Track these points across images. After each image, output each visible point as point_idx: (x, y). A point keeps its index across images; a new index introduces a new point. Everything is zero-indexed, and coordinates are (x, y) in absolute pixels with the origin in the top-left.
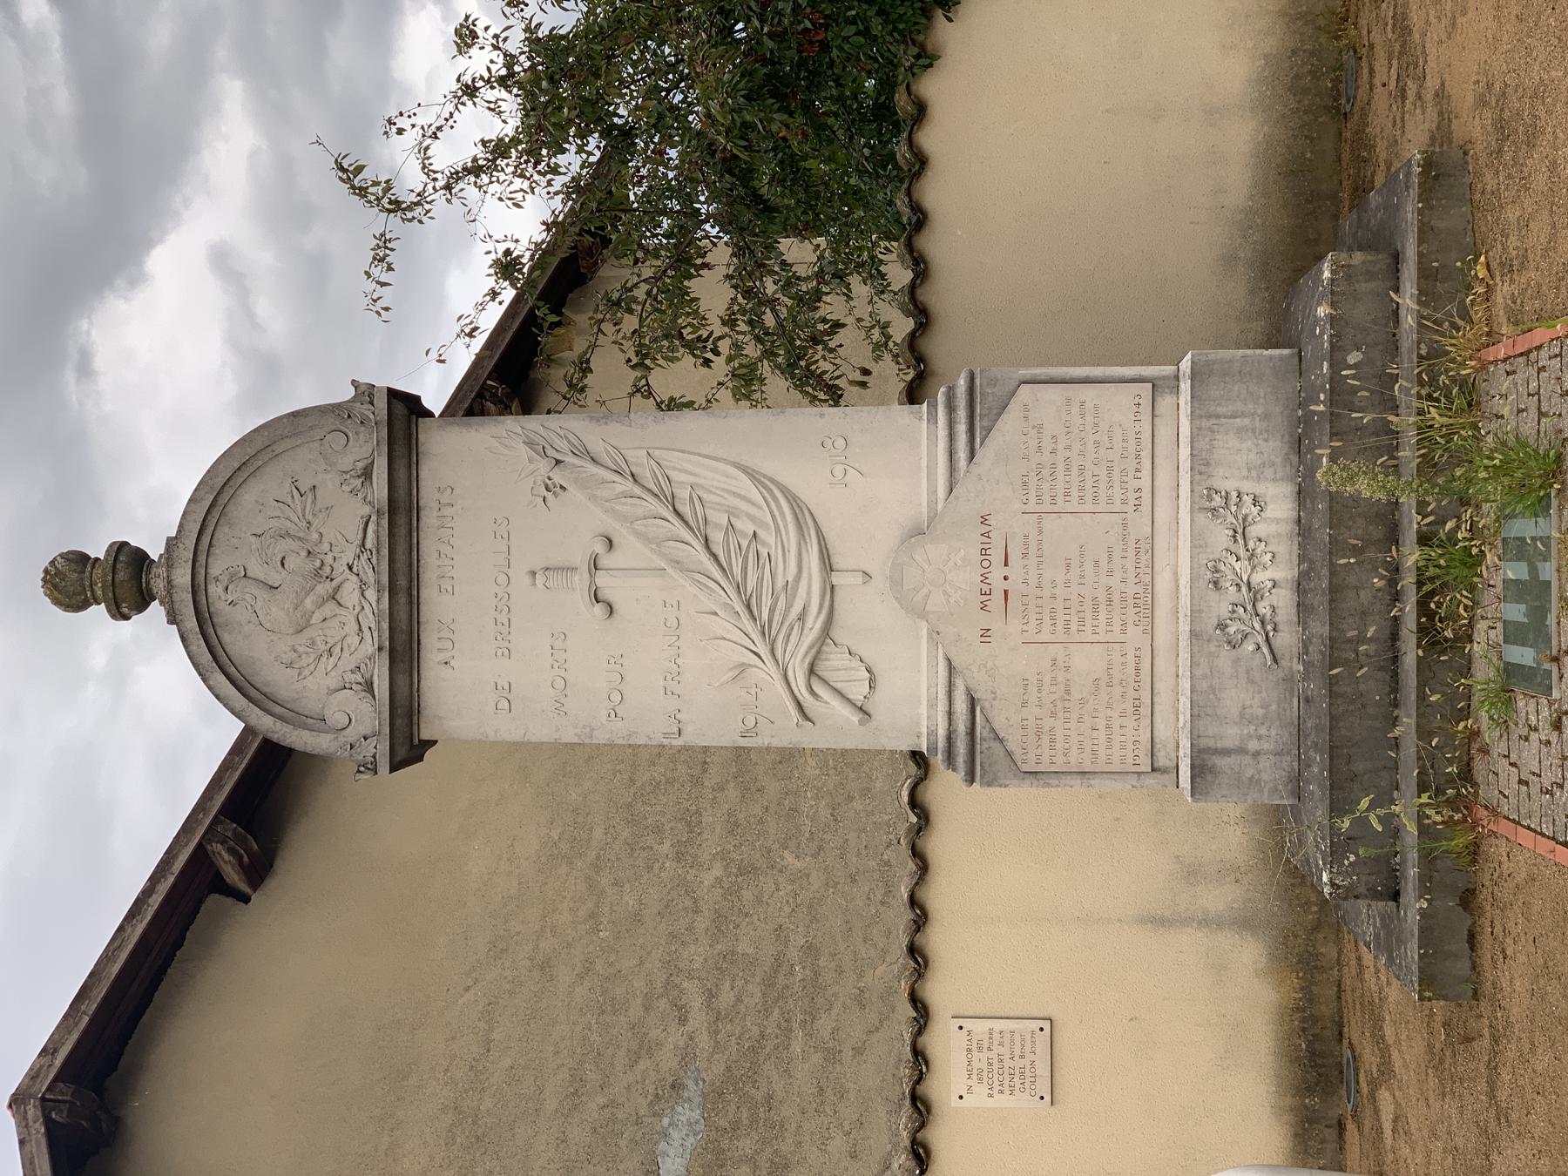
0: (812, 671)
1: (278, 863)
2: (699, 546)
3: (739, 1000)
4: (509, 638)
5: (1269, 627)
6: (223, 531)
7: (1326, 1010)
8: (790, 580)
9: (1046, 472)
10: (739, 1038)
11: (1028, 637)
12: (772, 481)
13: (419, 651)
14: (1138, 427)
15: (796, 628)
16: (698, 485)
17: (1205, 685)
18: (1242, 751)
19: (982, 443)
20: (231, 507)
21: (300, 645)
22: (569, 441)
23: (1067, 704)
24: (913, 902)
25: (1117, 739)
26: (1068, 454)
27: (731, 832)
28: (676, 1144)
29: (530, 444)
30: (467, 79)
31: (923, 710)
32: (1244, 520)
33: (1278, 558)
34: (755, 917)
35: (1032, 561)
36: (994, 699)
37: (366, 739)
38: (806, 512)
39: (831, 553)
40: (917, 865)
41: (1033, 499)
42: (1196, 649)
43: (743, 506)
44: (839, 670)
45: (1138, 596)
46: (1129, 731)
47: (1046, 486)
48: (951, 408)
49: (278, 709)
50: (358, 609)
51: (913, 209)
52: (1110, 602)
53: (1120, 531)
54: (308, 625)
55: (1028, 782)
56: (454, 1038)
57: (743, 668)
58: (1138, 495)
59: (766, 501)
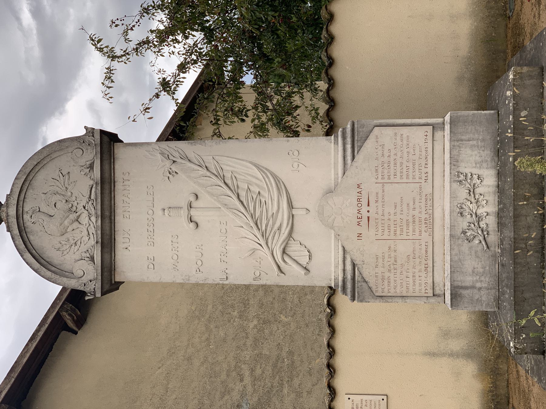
0: (284, 252)
1: (88, 319)
2: (235, 198)
3: (263, 372)
4: (153, 237)
5: (485, 233)
6: (30, 192)
7: (502, 391)
10: (263, 387)
11: (379, 237)
12: (266, 169)
13: (114, 243)
15: (277, 233)
16: (234, 171)
17: (456, 258)
18: (473, 287)
19: (358, 152)
20: (33, 181)
21: (63, 241)
22: (179, 153)
24: (329, 345)
25: (417, 282)
26: (395, 157)
27: (261, 307)
29: (162, 154)
30: (145, 6)
31: (333, 269)
32: (474, 186)
33: (489, 203)
34: (270, 340)
35: (380, 204)
36: (363, 264)
37: (91, 281)
38: (281, 183)
39: (292, 201)
40: (330, 330)
41: (380, 177)
42: (452, 242)
43: (254, 180)
44: (296, 251)
45: (427, 219)
46: (423, 278)
48: (344, 138)
49: (53, 269)
50: (88, 225)
51: (328, 58)
52: (414, 222)
53: (418, 191)
54: (66, 232)
55: (378, 300)
56: (154, 387)
57: (254, 250)
58: (426, 175)
59: (264, 179)
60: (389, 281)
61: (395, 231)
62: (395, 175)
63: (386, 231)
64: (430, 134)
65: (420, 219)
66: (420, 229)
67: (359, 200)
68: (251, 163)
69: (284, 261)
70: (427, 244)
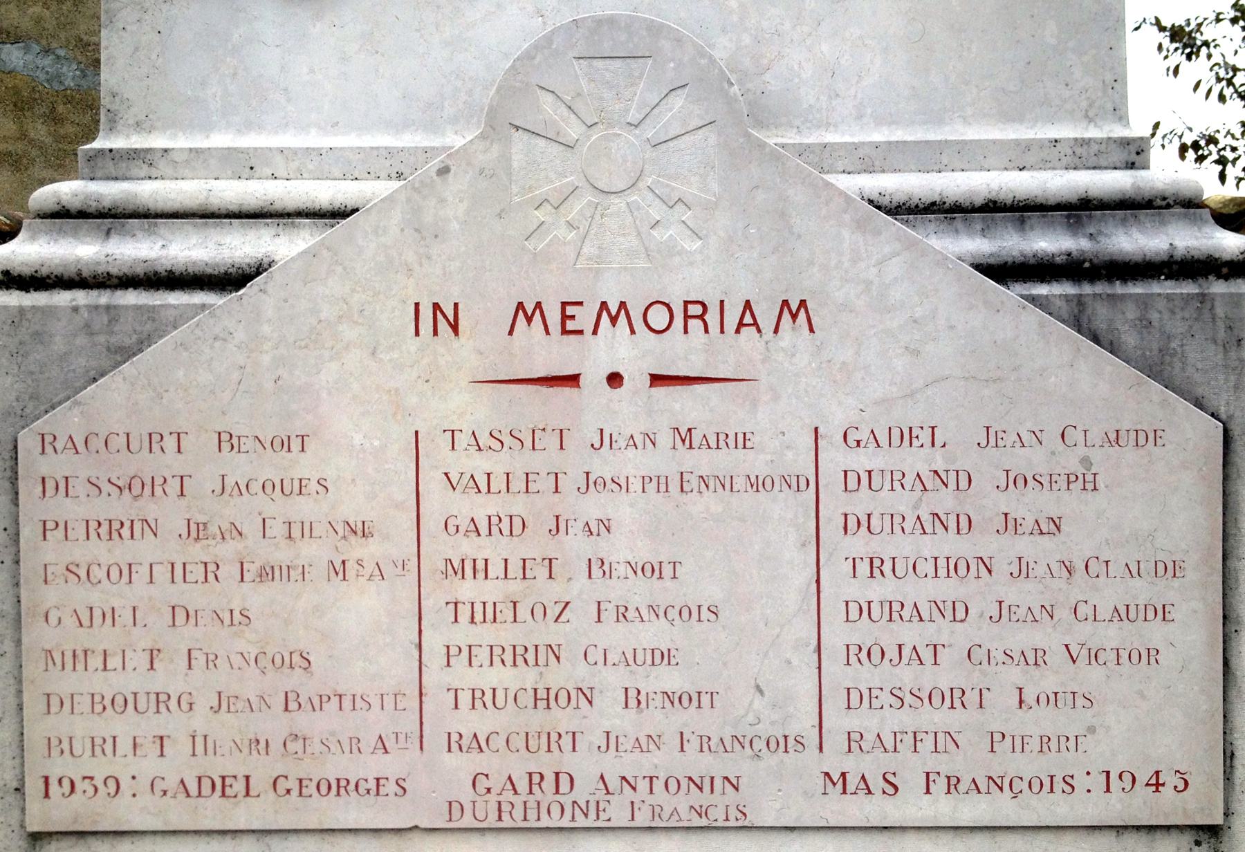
9: (945, 501)
11: (438, 456)
14: (1087, 782)
19: (1032, 299)
23: (229, 571)
25: (122, 726)
26: (1002, 567)
28: (38, 61)
31: (220, 140)
41: (862, 461)
46: (149, 765)
47: (902, 502)
53: (764, 729)
58: (877, 783)
60: (126, 532)
61: (480, 565)
62: (875, 566)
65: (566, 741)
66: (499, 742)
70: (391, 788)
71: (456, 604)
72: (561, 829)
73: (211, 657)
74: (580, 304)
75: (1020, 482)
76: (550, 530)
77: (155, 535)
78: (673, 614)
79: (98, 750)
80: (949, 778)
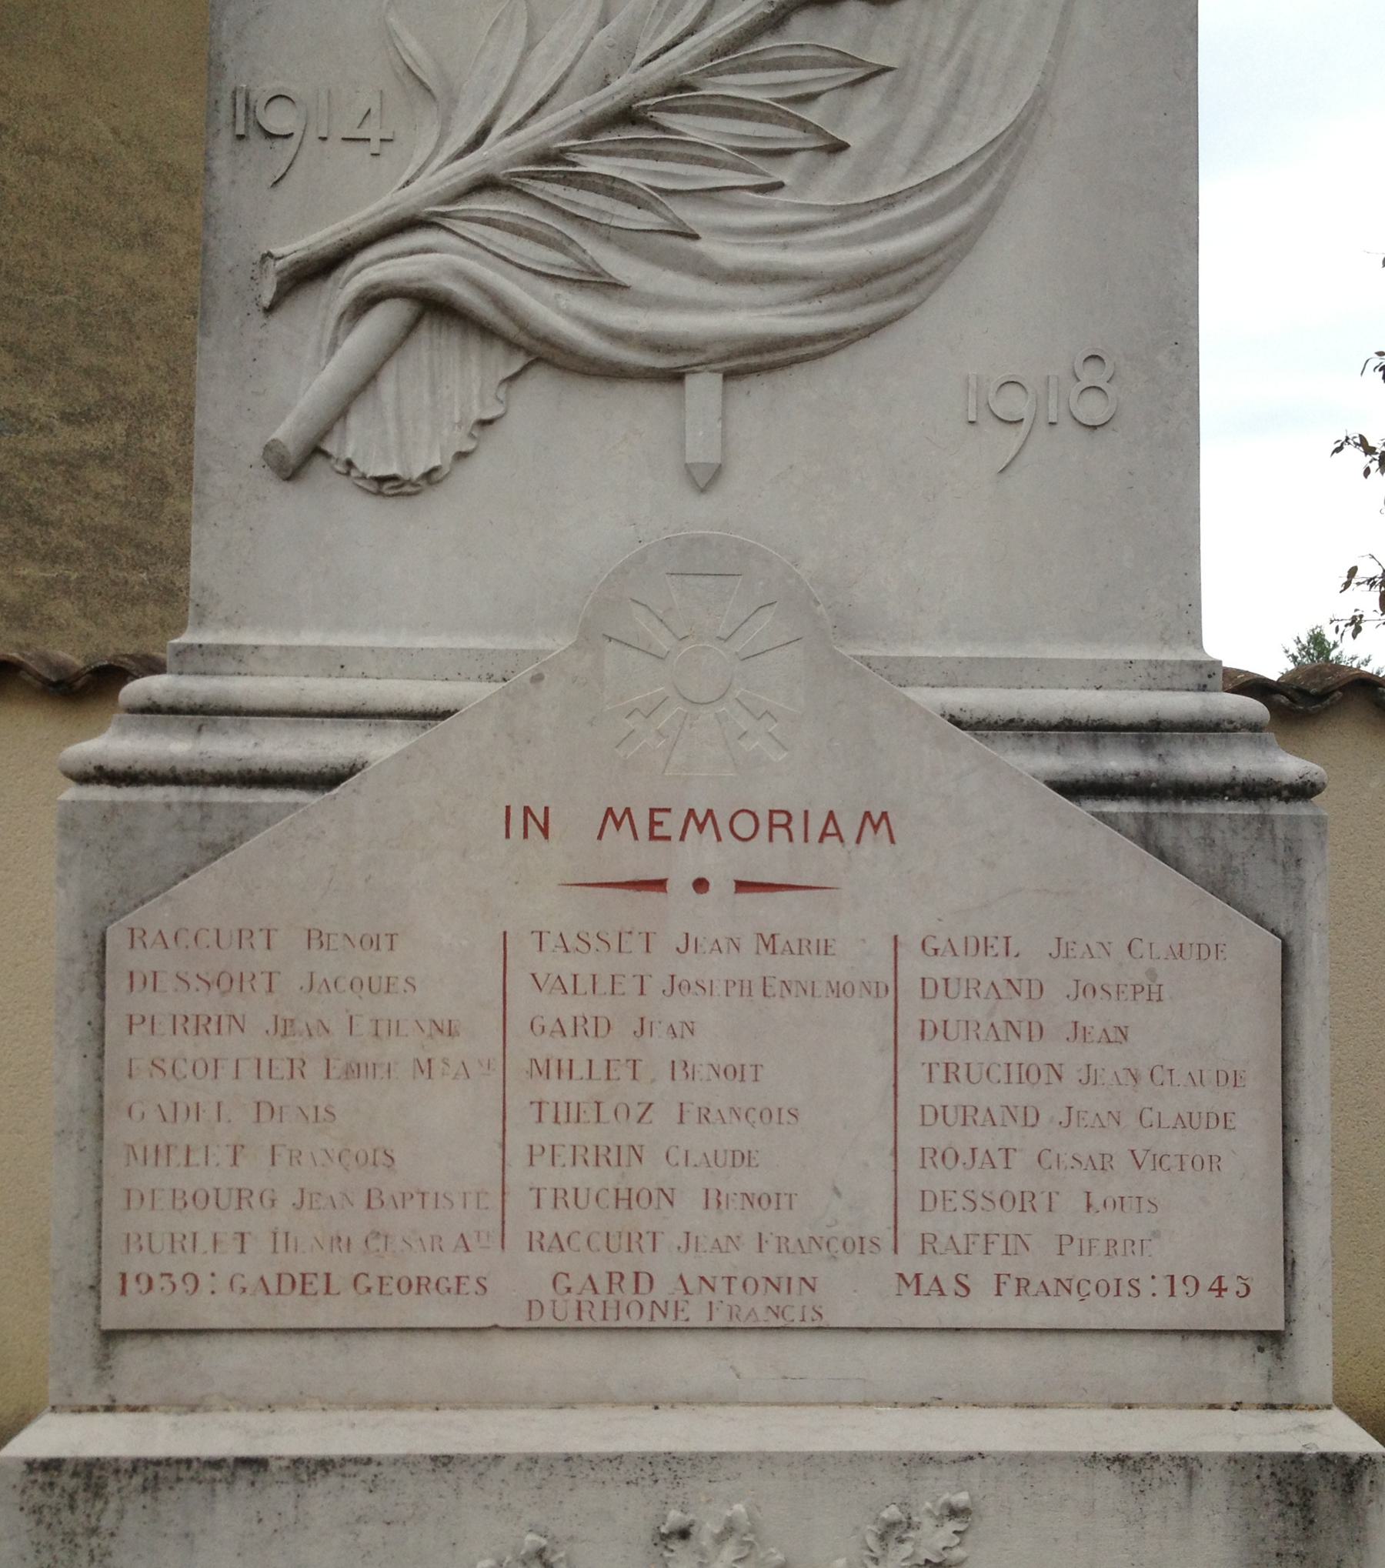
8: (699, 246)
9: (1017, 1009)
12: (991, 208)
19: (1102, 817)
25: (202, 1222)
31: (310, 638)
38: (896, 304)
39: (780, 377)
41: (939, 968)
43: (924, 114)
47: (977, 1009)
52: (626, 1199)
58: (948, 1285)
59: (935, 181)
60: (213, 1027)
61: (565, 1065)
63: (568, 1008)
64: (1232, 1312)
65: (647, 1242)
66: (579, 1242)
67: (780, 821)
68: (1039, 103)
69: (367, 302)
70: (470, 1286)
71: (540, 1103)
72: (640, 1329)
73: (295, 1153)
74: (668, 810)
75: (1089, 992)
76: (635, 1032)
77: (242, 1030)
78: (754, 1116)
79: (177, 1246)
80: (1019, 1280)
